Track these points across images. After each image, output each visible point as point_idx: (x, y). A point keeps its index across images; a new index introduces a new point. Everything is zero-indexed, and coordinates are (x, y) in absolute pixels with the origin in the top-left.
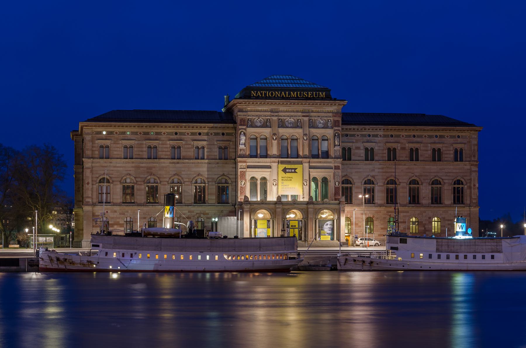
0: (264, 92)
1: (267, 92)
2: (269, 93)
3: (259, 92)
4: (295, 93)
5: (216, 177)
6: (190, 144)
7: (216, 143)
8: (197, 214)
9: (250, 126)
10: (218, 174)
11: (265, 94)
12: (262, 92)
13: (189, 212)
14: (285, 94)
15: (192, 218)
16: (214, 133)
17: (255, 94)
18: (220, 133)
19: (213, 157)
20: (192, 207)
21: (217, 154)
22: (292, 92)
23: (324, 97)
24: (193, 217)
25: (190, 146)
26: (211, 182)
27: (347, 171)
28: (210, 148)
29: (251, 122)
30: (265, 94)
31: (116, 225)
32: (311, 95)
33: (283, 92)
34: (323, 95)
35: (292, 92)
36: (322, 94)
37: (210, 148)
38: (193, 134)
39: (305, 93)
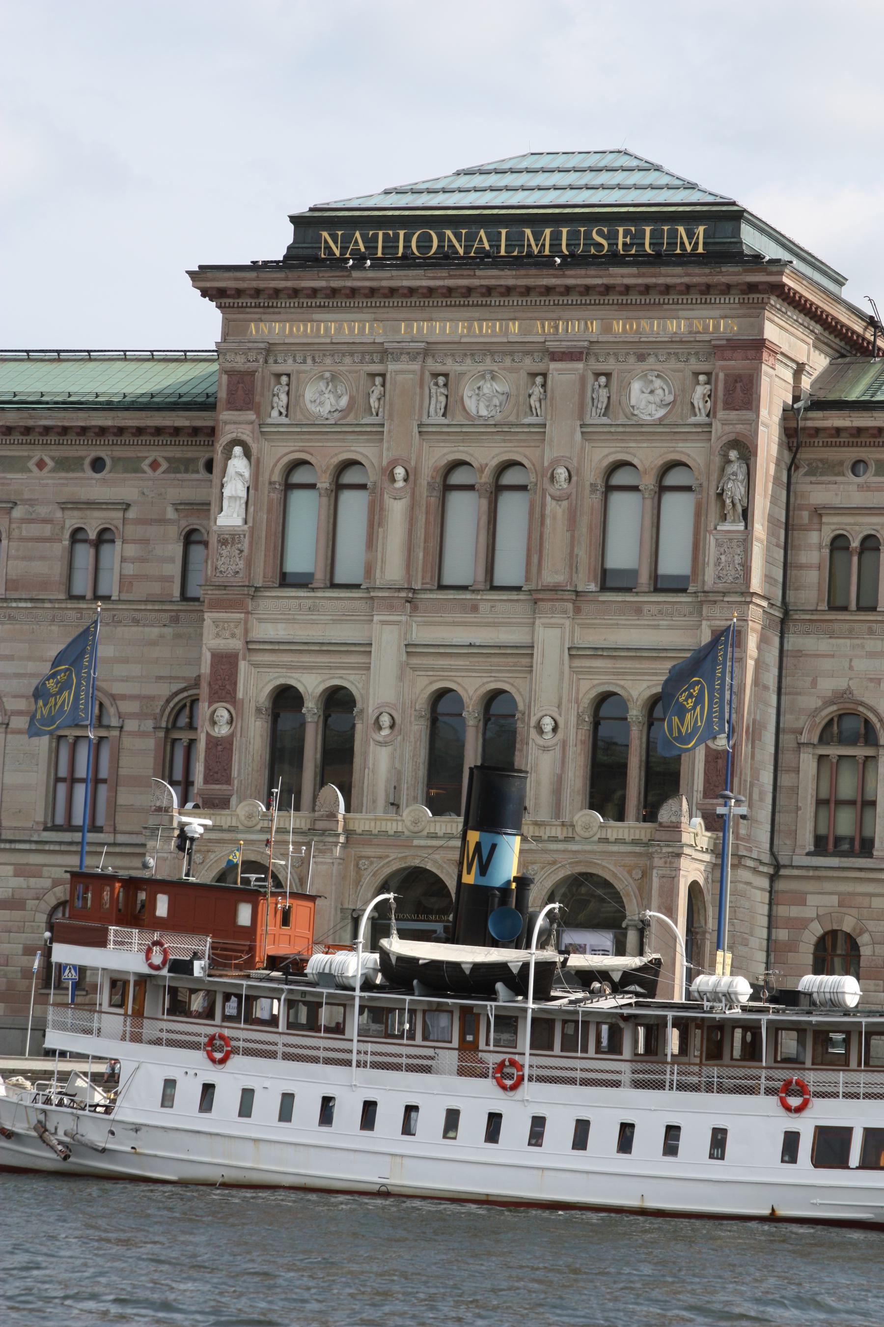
0: (386, 236)
1: (402, 233)
2: (407, 239)
3: (357, 234)
4: (548, 232)
5: (164, 690)
6: (45, 521)
7: (171, 514)
8: (56, 883)
9: (281, 413)
10: (172, 679)
11: (391, 243)
12: (376, 236)
13: (20, 871)
14: (494, 240)
15: (31, 904)
16: (168, 459)
17: (336, 242)
18: (194, 460)
19: (156, 588)
20: (33, 847)
21: (175, 569)
22: (528, 232)
23: (700, 250)
24: (37, 899)
25: (47, 530)
26: (132, 716)
27: (851, 668)
28: (145, 541)
29: (288, 394)
30: (391, 243)
31: (377, 985)
32: (632, 245)
33: (482, 233)
34: (697, 244)
35: (528, 232)
36: (690, 234)
37: (145, 541)
38: (63, 464)
39: (600, 233)
